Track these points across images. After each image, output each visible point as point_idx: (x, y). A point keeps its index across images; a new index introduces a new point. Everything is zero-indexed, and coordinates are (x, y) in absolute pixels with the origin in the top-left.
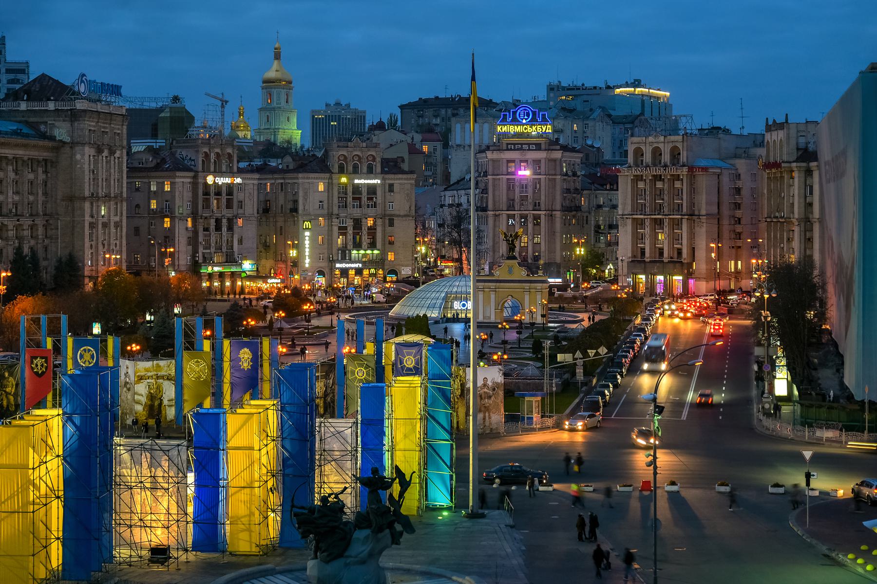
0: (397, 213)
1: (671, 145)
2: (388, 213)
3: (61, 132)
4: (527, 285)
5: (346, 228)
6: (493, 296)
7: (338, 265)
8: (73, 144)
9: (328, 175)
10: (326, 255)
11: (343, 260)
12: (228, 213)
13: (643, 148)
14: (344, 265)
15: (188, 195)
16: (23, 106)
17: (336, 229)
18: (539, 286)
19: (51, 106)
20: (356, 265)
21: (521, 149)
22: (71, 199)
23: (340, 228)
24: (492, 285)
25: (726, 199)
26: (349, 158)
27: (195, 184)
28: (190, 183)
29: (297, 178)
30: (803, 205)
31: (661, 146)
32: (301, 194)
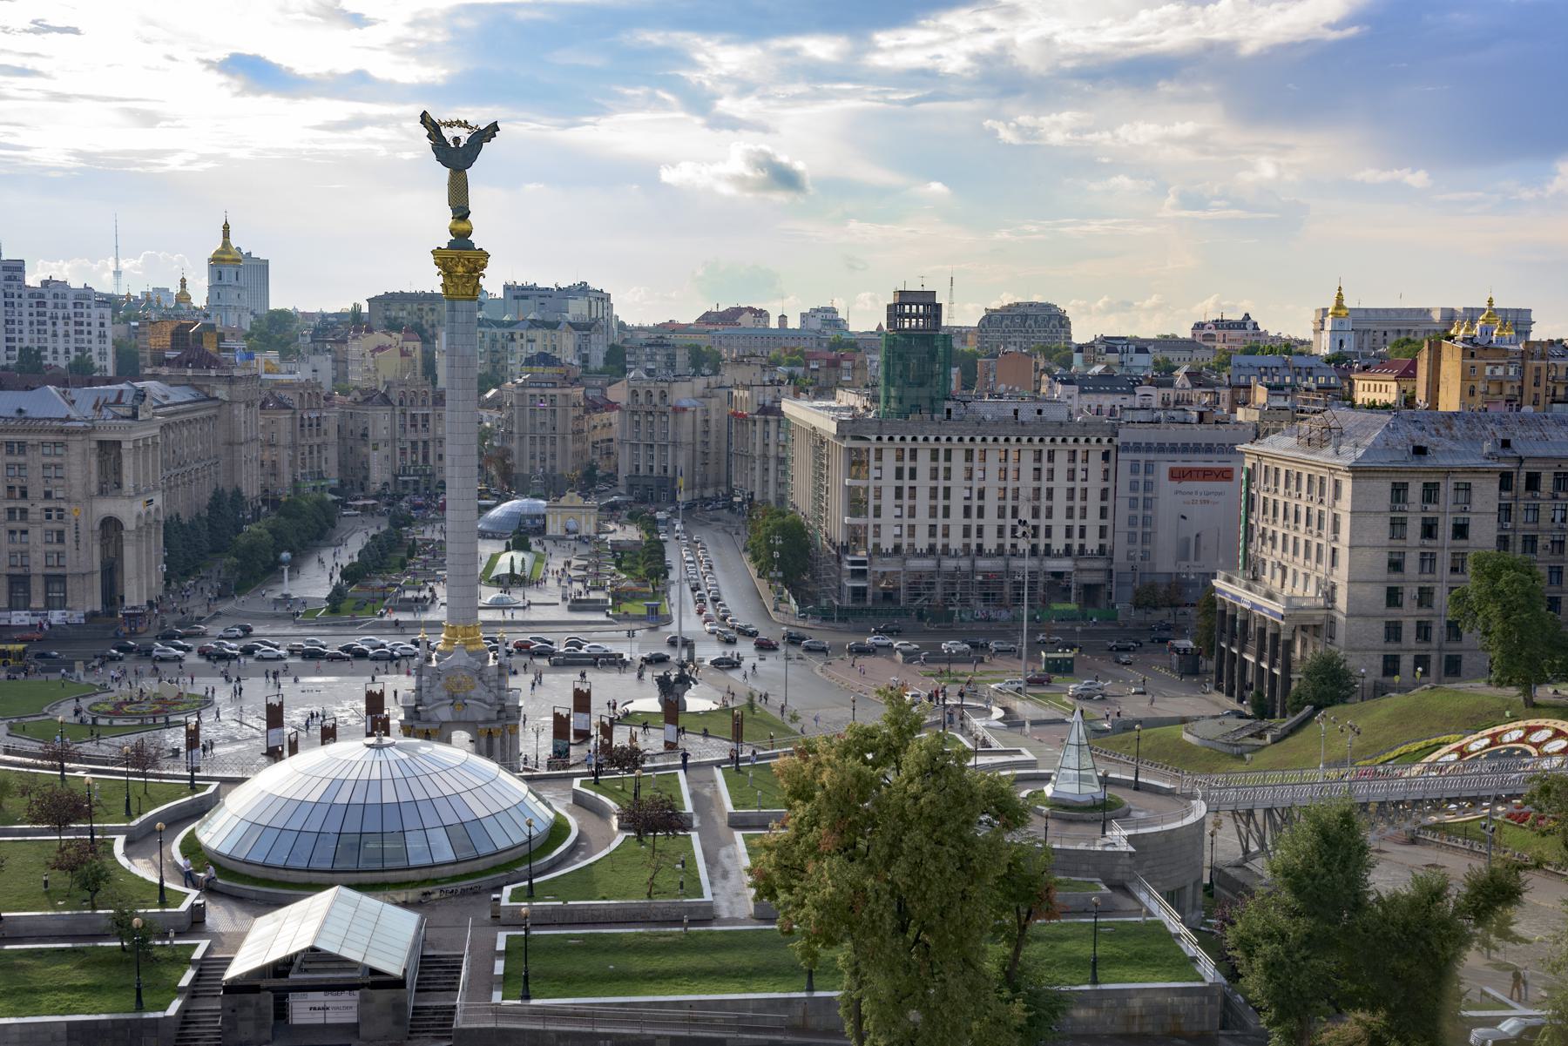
3: (221, 392)
8: (231, 403)
12: (318, 441)
15: (289, 428)
16: (190, 372)
19: (213, 373)
22: (231, 444)
25: (699, 428)
27: (293, 419)
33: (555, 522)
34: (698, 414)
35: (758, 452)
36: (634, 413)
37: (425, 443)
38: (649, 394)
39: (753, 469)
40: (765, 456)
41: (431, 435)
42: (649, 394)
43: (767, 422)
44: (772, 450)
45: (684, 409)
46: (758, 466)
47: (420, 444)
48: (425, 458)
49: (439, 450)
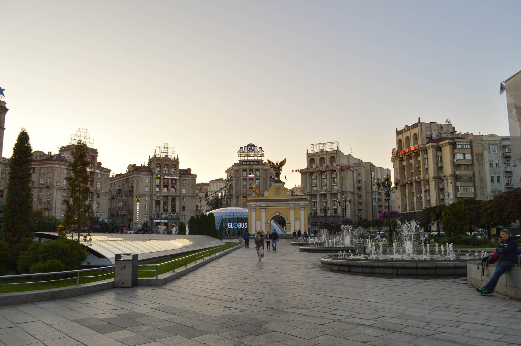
0: (187, 195)
1: (330, 156)
2: (182, 194)
4: (292, 204)
5: (159, 201)
6: (263, 213)
7: (154, 221)
9: (150, 173)
10: (148, 216)
11: (158, 218)
13: (315, 158)
14: (158, 221)
17: (154, 202)
18: (302, 203)
20: (165, 221)
21: (250, 164)
23: (156, 201)
24: (263, 204)
26: (162, 165)
28: (66, 169)
29: (133, 174)
30: (436, 168)
31: (324, 156)
32: (135, 182)
33: (258, 219)
34: (355, 175)
35: (432, 172)
36: (312, 173)
37: (174, 199)
38: (322, 159)
39: (427, 191)
40: (439, 179)
41: (178, 194)
42: (322, 159)
43: (439, 149)
44: (448, 170)
45: (348, 167)
46: (433, 186)
47: (170, 198)
48: (174, 205)
49: (183, 204)
